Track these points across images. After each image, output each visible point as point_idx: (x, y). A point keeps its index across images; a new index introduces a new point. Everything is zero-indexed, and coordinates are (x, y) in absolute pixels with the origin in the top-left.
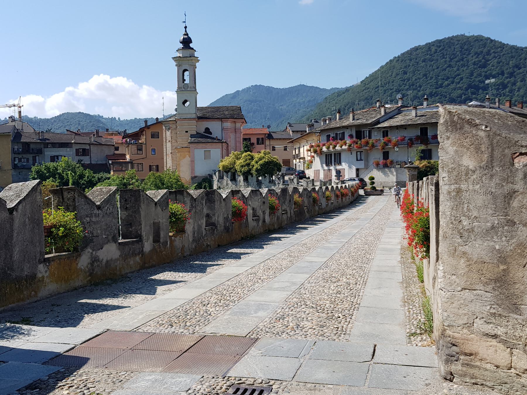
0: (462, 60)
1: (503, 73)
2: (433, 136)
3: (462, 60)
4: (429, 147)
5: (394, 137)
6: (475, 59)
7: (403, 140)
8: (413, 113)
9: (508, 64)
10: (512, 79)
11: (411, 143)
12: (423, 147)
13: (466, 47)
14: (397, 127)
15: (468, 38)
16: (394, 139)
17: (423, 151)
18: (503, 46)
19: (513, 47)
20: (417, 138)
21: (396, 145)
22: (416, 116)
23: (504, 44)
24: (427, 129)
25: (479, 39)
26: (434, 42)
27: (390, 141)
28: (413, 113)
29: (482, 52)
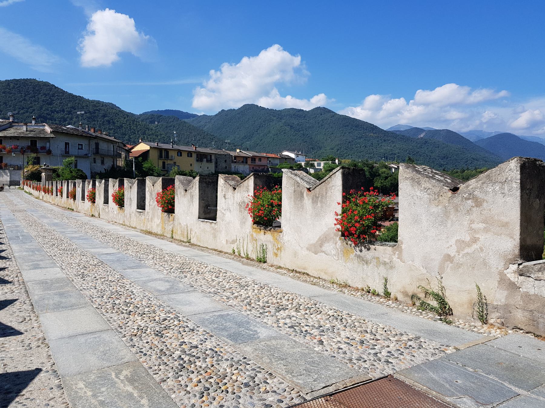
0: (34, 97)
1: (63, 111)
2: (41, 147)
3: (34, 97)
4: (39, 156)
5: (8, 145)
6: (43, 98)
7: (16, 148)
8: (24, 128)
9: (67, 105)
10: (70, 116)
11: (23, 151)
12: (34, 155)
13: (37, 88)
14: (11, 138)
15: (39, 82)
16: (8, 148)
17: (35, 158)
18: (63, 92)
19: (71, 95)
20: (28, 148)
21: (10, 152)
22: (27, 131)
23: (64, 91)
24: (36, 141)
25: (46, 85)
26: (13, 80)
27: (5, 148)
28: (24, 128)
29: (49, 94)
